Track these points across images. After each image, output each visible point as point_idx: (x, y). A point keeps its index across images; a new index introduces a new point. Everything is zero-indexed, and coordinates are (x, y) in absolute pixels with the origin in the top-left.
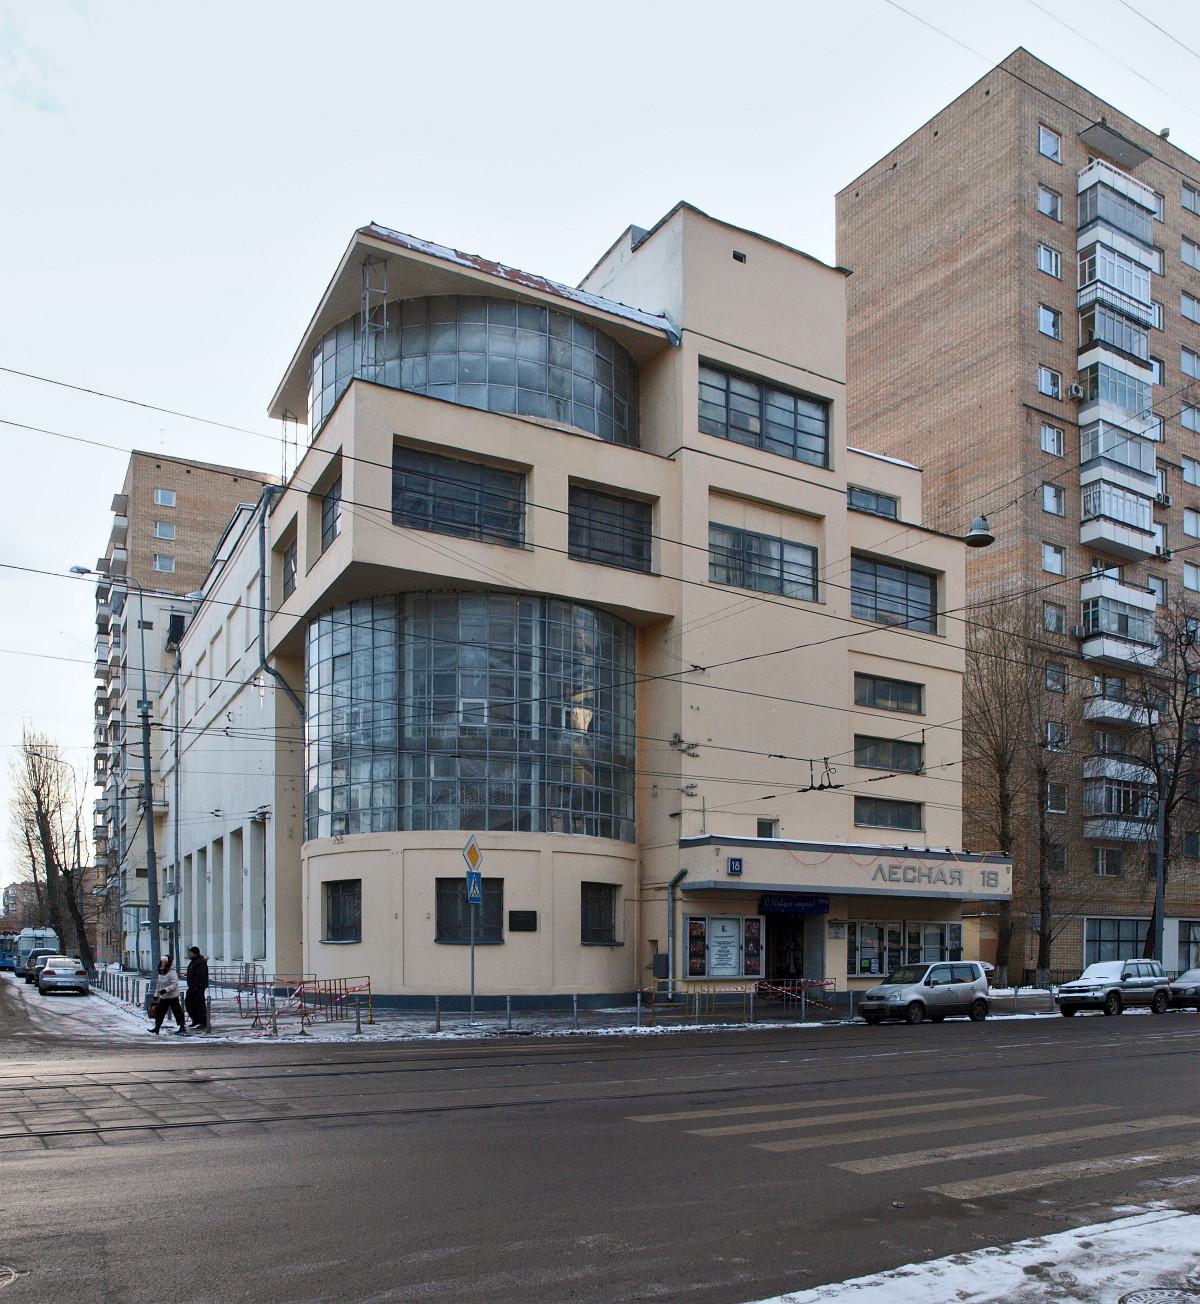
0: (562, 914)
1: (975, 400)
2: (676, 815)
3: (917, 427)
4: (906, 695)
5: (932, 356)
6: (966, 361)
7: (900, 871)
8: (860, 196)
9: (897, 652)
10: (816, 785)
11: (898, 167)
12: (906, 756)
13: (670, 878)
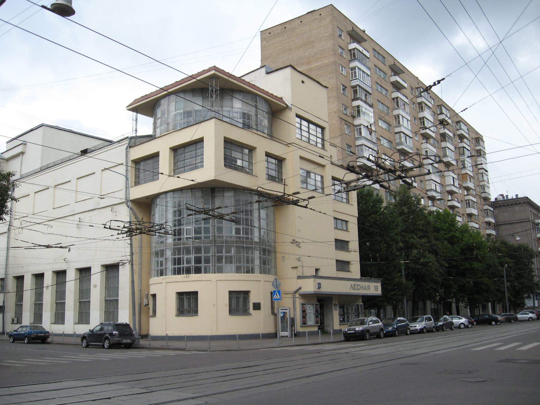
13: (295, 290)
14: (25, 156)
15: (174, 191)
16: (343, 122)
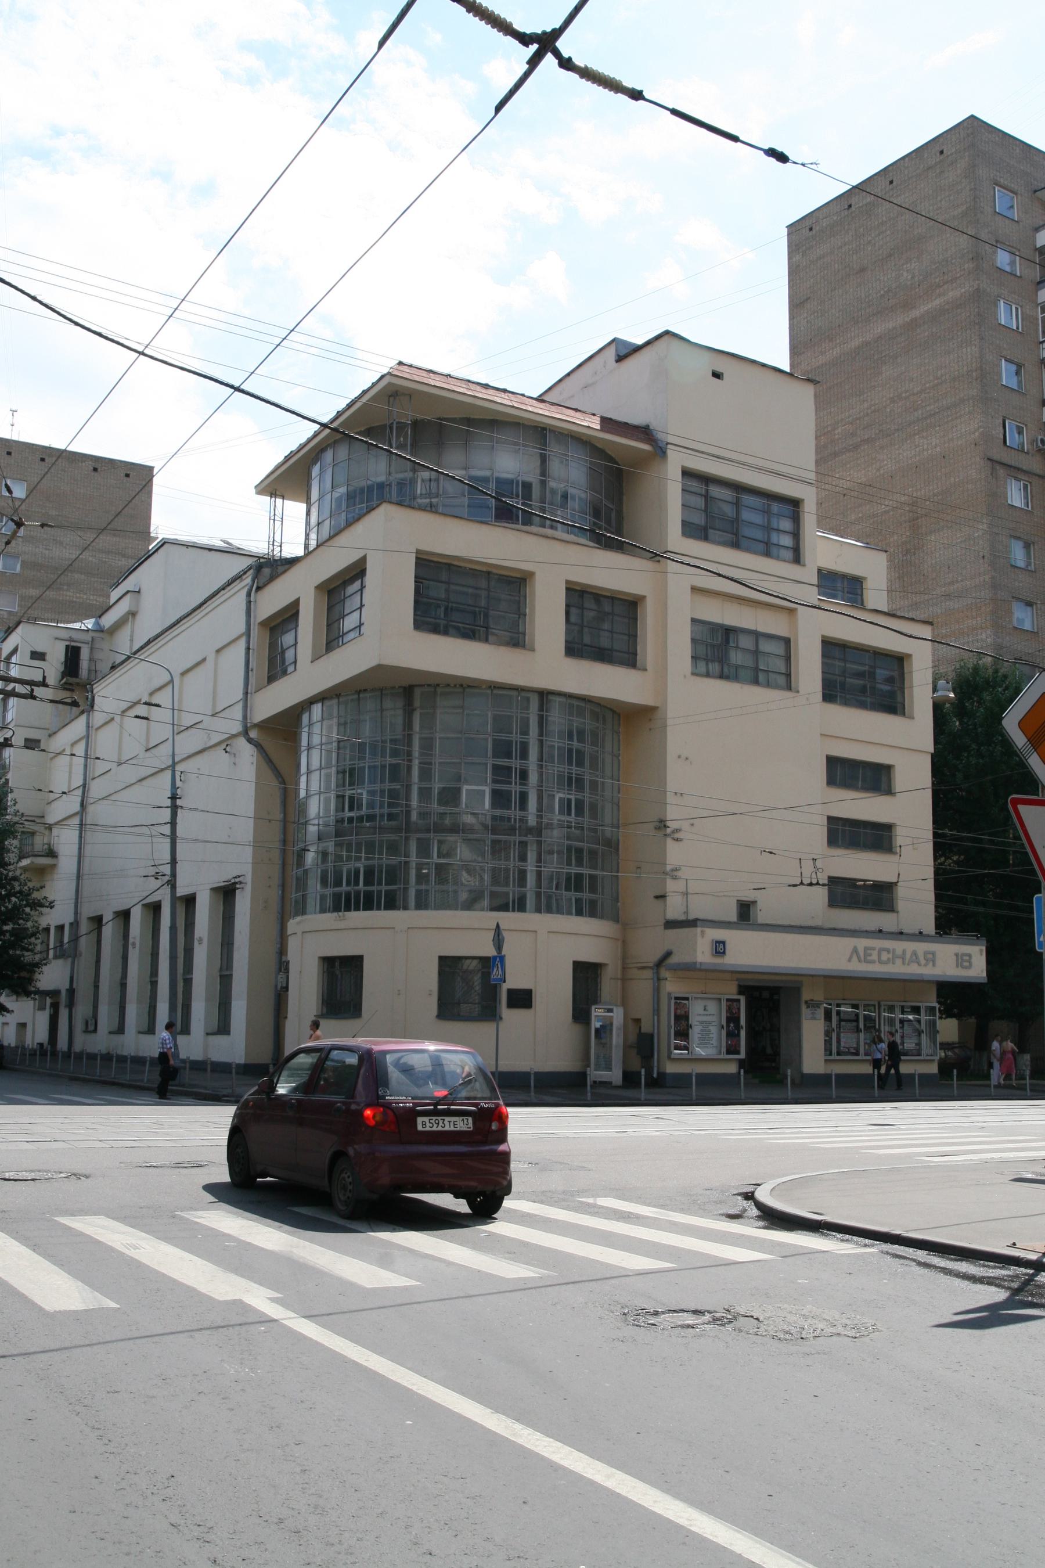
0: (555, 993)
1: (938, 449)
2: (662, 897)
3: (879, 470)
4: (874, 777)
5: (892, 400)
6: (928, 408)
7: (875, 954)
8: (814, 232)
9: (865, 732)
10: (806, 882)
11: (853, 208)
12: (877, 837)
14: (138, 617)
15: (322, 698)
16: (1001, 472)
